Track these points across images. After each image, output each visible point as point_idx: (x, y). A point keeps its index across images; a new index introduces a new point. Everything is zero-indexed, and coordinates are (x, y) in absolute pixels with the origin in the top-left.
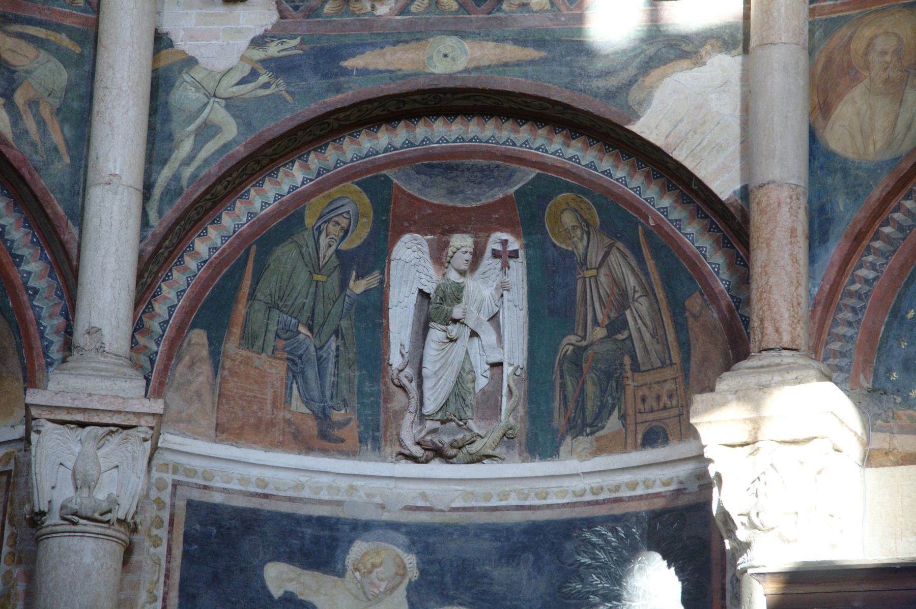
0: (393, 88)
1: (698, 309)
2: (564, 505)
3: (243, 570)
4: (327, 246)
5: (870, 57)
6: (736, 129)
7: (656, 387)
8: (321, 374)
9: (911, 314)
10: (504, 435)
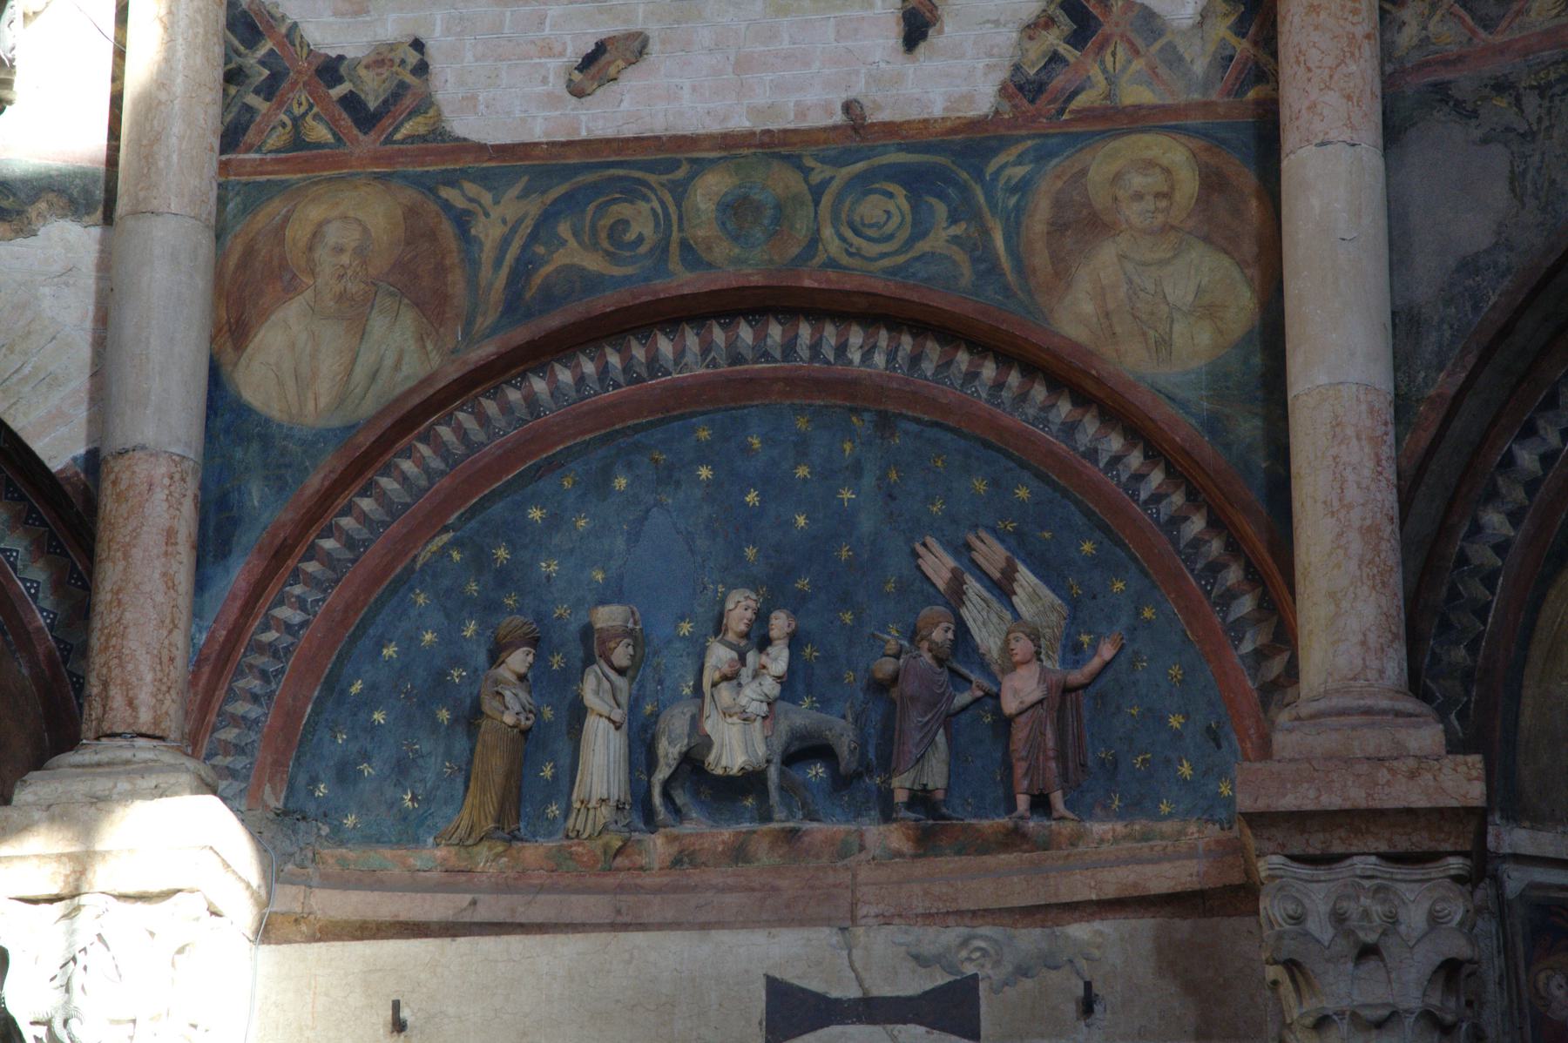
5: (316, 256)
6: (84, 352)
9: (357, 687)
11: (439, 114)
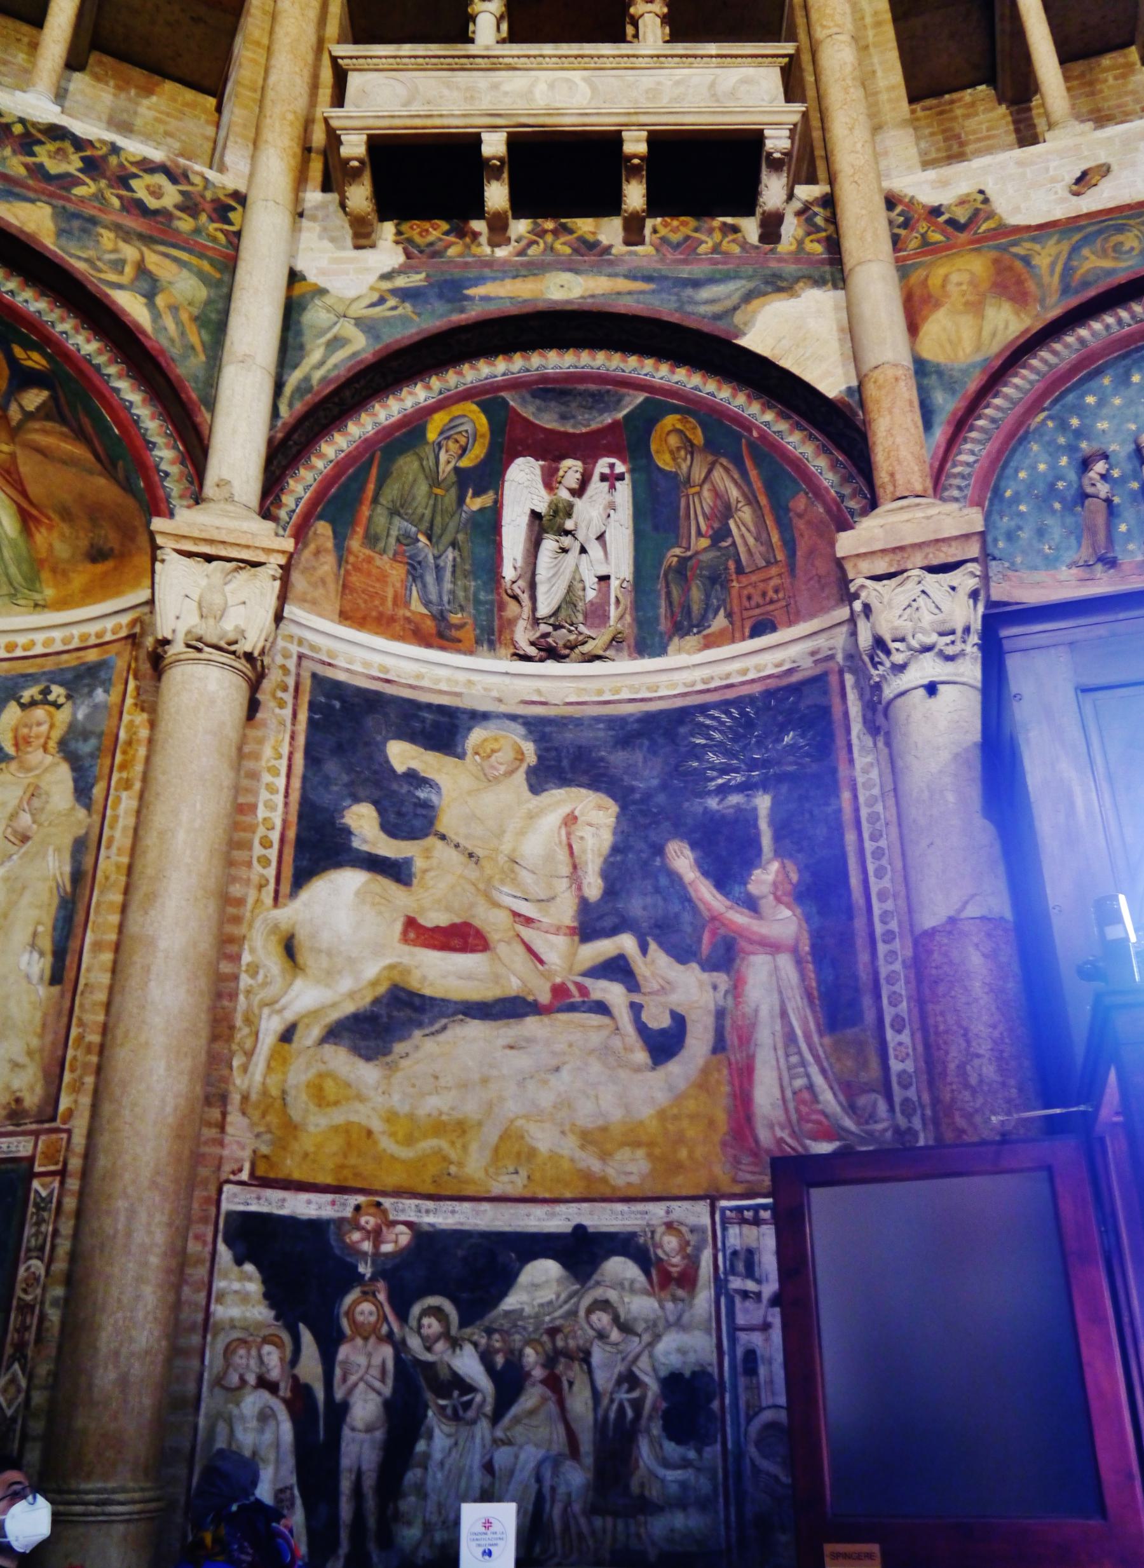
0: (514, 310)
1: (802, 507)
2: (675, 696)
3: (367, 744)
4: (446, 463)
7: (761, 585)
8: (439, 579)
9: (1008, 493)
10: (613, 639)
11: (1001, 218)
